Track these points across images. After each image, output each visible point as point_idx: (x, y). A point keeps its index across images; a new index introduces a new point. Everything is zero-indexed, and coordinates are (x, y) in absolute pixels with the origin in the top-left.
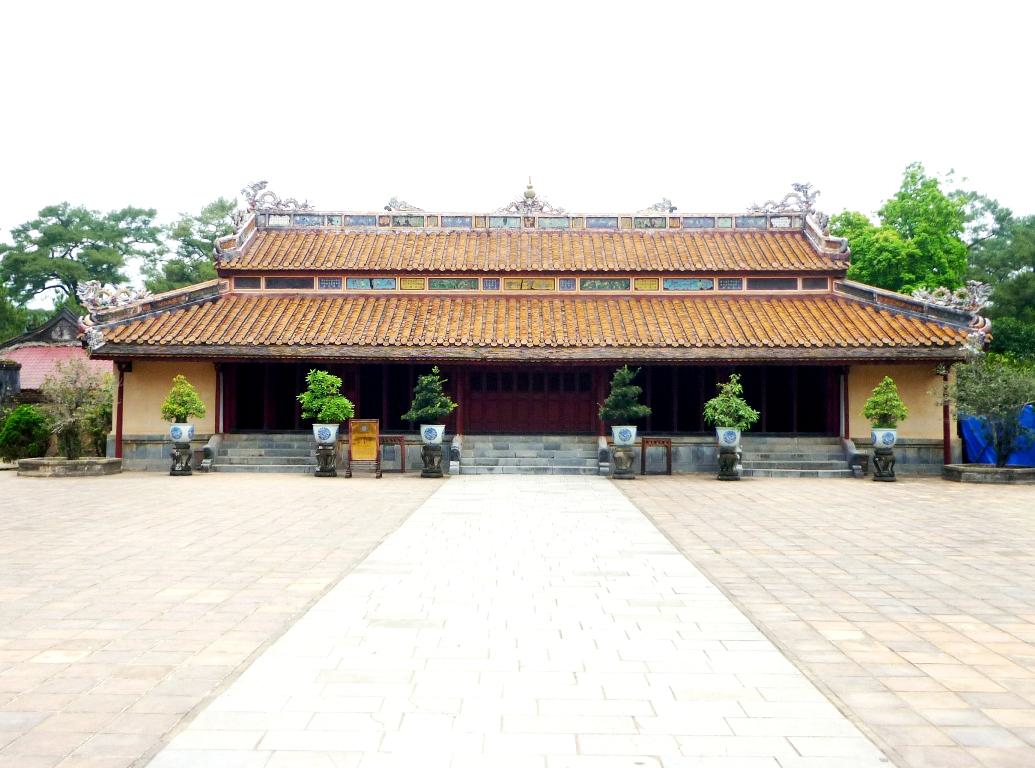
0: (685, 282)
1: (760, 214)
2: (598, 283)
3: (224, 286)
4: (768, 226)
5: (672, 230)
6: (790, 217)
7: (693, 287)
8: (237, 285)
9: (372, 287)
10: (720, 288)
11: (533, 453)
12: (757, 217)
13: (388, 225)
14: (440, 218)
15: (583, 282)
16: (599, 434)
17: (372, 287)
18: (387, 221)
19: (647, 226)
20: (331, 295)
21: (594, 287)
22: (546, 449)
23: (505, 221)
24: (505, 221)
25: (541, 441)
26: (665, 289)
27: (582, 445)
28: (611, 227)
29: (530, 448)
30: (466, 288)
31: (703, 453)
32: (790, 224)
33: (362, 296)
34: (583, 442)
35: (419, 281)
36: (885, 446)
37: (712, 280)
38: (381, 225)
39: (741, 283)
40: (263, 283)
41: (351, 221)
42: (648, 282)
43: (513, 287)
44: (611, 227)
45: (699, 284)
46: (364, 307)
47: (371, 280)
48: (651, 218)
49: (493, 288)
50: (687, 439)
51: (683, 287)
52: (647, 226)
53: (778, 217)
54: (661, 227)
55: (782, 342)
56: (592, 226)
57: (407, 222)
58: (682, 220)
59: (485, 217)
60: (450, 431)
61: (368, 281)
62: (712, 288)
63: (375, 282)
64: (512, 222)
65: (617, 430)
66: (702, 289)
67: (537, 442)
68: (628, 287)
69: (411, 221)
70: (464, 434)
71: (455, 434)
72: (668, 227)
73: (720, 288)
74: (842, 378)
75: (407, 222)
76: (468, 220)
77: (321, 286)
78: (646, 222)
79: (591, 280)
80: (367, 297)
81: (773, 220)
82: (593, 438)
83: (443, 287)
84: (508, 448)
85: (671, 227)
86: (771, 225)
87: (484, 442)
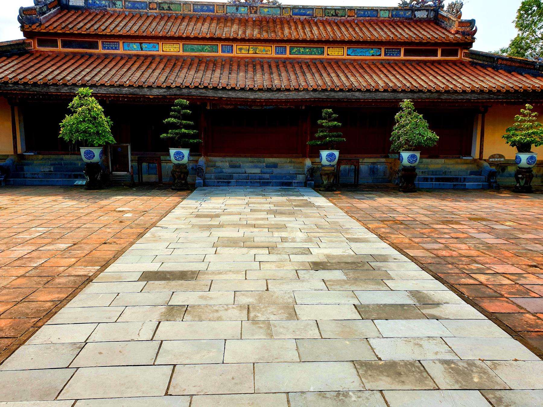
0: (362, 50)
1: (408, 8)
2: (302, 50)
3: (30, 44)
4: (413, 17)
5: (349, 19)
6: (427, 10)
7: (367, 54)
8: (39, 45)
9: (142, 50)
10: (386, 55)
11: (258, 171)
12: (405, 10)
13: (156, 9)
14: (192, 5)
15: (291, 48)
16: (305, 156)
17: (142, 50)
18: (155, 6)
19: (332, 15)
20: (112, 54)
21: (299, 53)
22: (267, 166)
23: (237, 9)
24: (237, 9)
25: (264, 162)
26: (348, 55)
27: (293, 164)
28: (308, 15)
29: (256, 167)
30: (209, 51)
31: (377, 169)
32: (427, 15)
33: (135, 55)
34: (294, 162)
35: (175, 46)
36: (528, 166)
37: (381, 49)
38: (150, 9)
39: (400, 52)
40: (59, 43)
41: (130, 5)
42: (337, 49)
43: (243, 51)
44: (308, 15)
45: (372, 52)
46: (135, 62)
47: (141, 43)
48: (335, 10)
49: (228, 52)
50: (366, 160)
51: (360, 54)
52: (332, 15)
53: (420, 10)
54: (342, 16)
55: (442, 89)
56: (296, 14)
57: (169, 7)
58: (356, 11)
59: (223, 6)
60: (195, 151)
61: (139, 44)
62: (380, 55)
63: (144, 46)
64: (242, 10)
65: (324, 153)
66: (373, 55)
67: (260, 162)
68: (323, 53)
69: (172, 7)
70: (206, 155)
71: (201, 156)
72: (346, 16)
73: (386, 55)
74: (480, 116)
75: (169, 7)
76: (211, 7)
77: (104, 48)
78: (332, 12)
79: (297, 47)
80: (138, 56)
81: (416, 13)
82: (300, 160)
83: (193, 50)
84: (239, 167)
85: (348, 16)
86: (415, 16)
87: (222, 161)
